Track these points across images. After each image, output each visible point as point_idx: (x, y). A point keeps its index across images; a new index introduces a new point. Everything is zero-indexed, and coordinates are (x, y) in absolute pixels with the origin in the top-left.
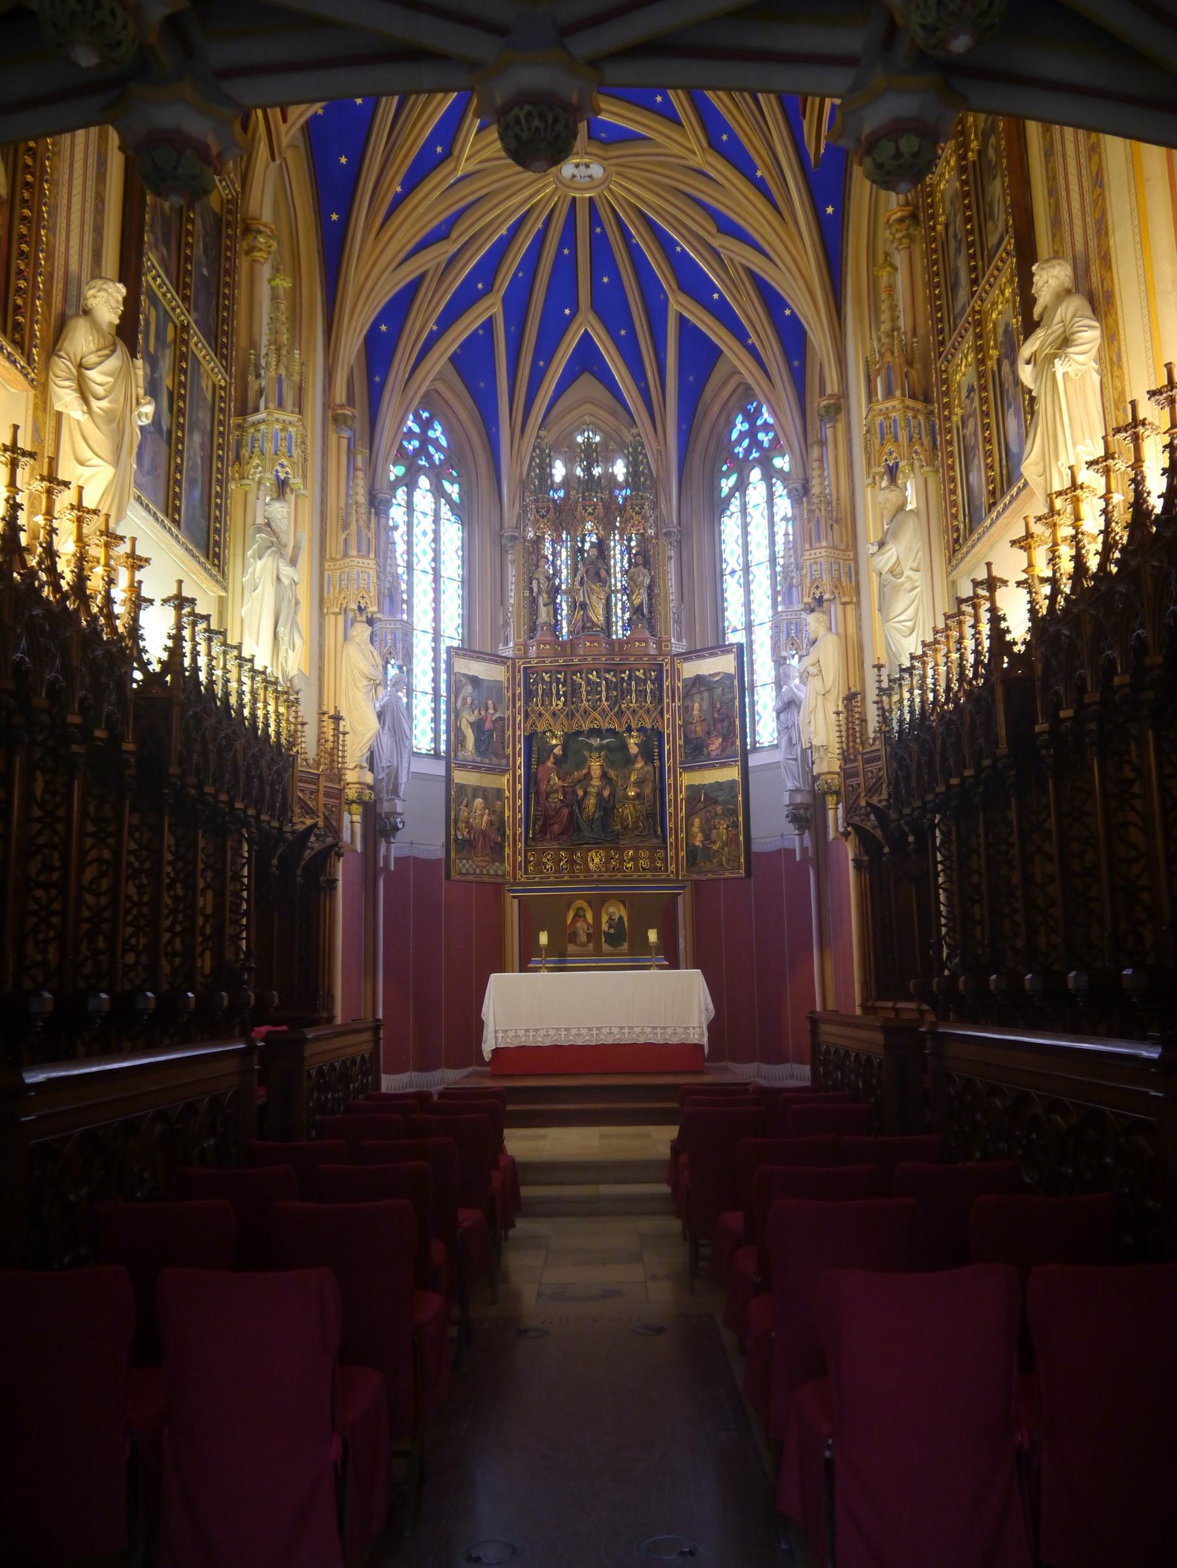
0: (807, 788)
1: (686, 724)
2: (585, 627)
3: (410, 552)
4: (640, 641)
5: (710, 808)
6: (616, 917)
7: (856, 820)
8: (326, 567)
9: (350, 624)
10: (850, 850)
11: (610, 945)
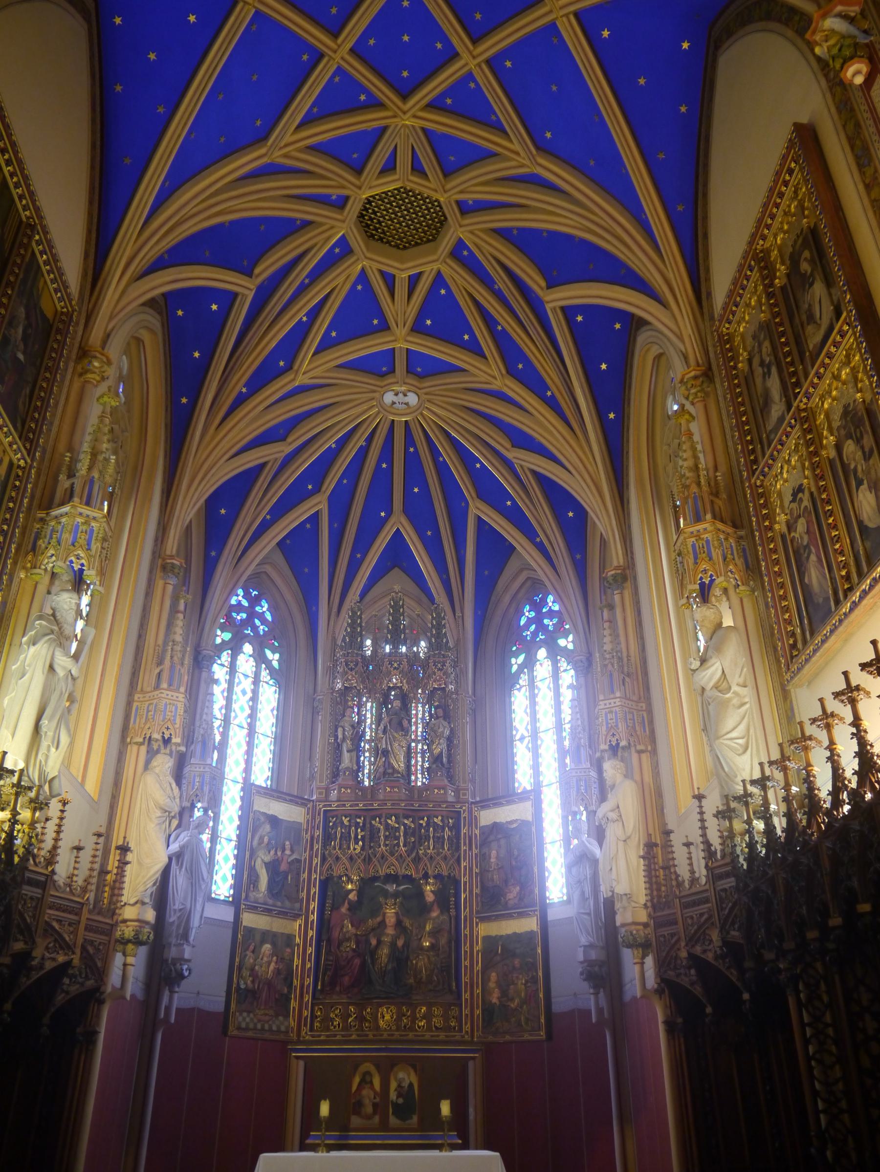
0: (601, 944)
2: (385, 774)
3: (228, 706)
4: (439, 789)
6: (405, 1084)
8: (136, 698)
9: (152, 754)
11: (398, 1117)
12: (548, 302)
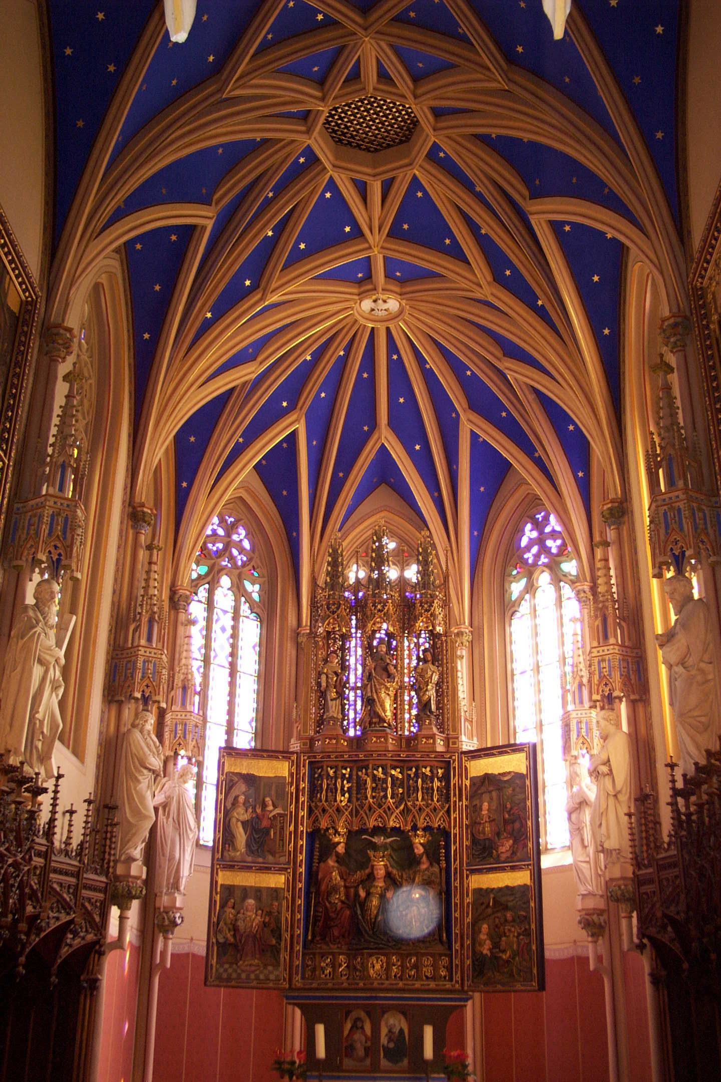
0: (600, 893)
1: (474, 824)
3: (207, 646)
5: (499, 914)
7: (653, 931)
10: (645, 963)
11: (389, 1060)
12: (531, 214)
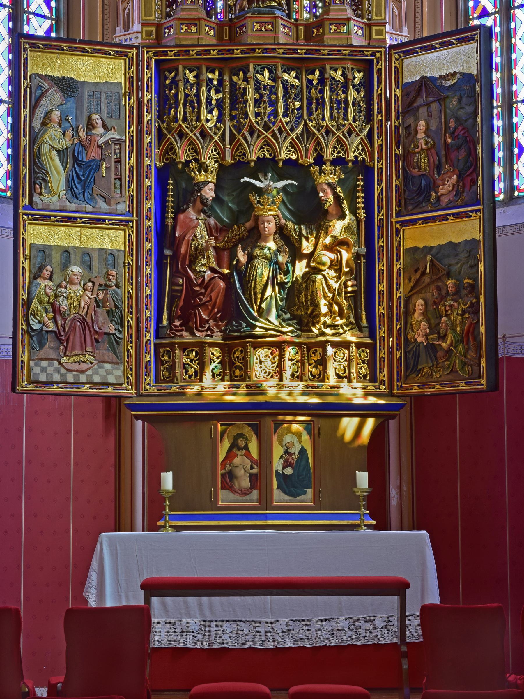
6: (295, 450)
